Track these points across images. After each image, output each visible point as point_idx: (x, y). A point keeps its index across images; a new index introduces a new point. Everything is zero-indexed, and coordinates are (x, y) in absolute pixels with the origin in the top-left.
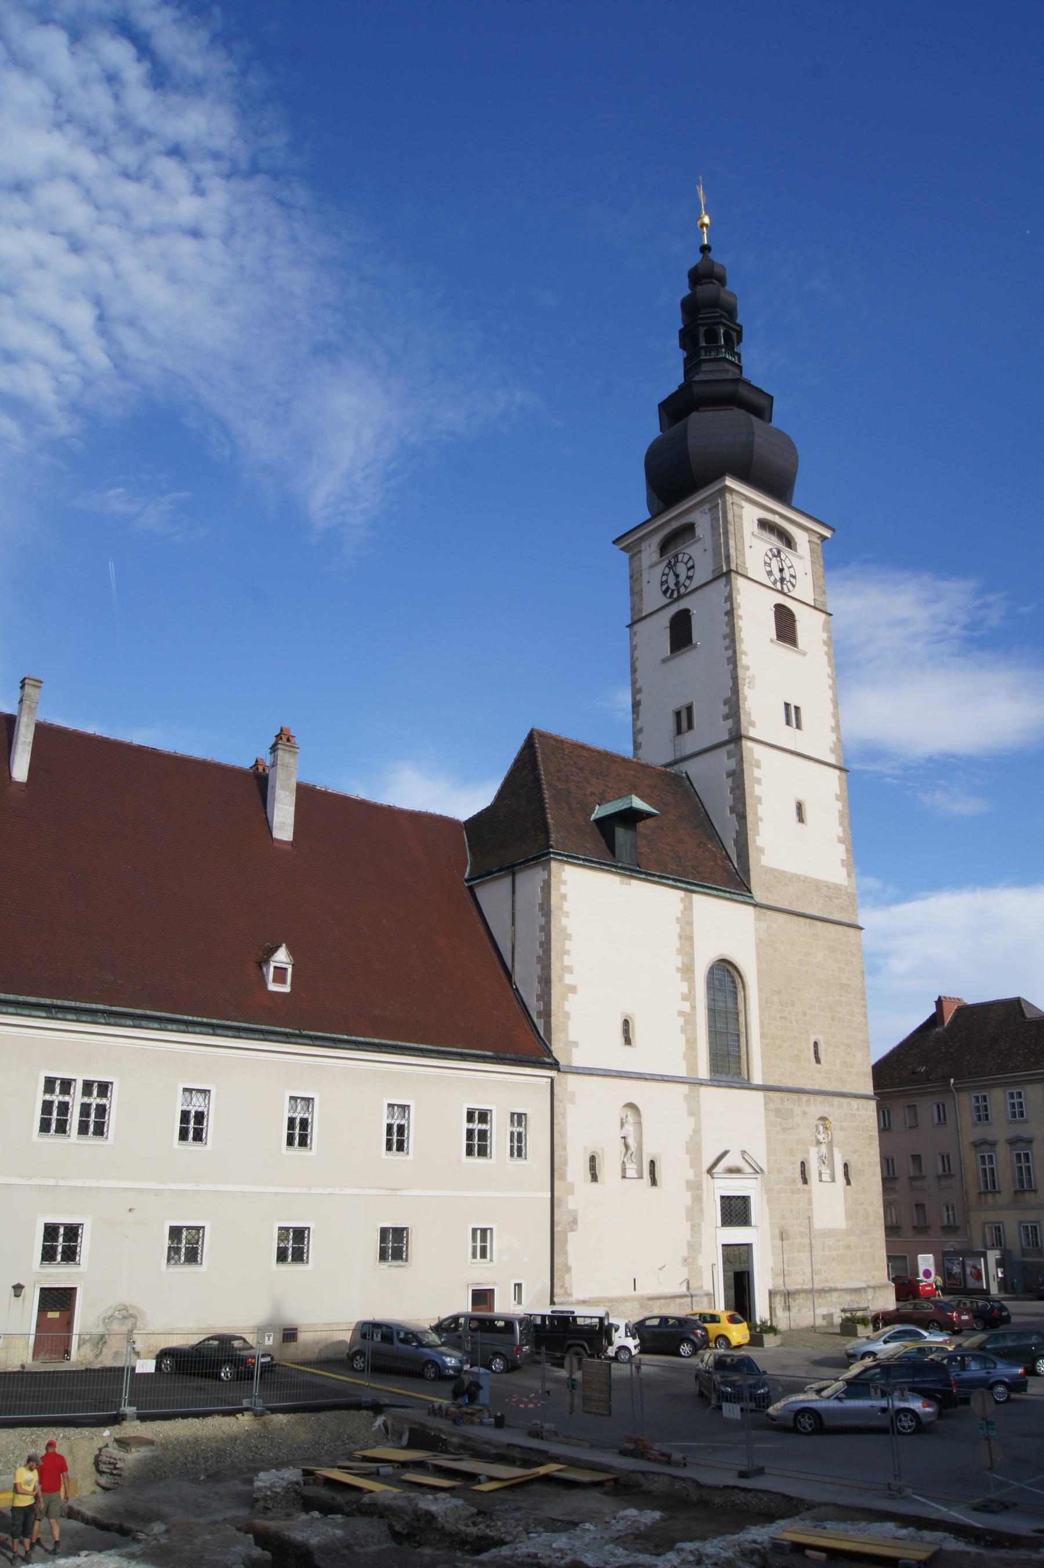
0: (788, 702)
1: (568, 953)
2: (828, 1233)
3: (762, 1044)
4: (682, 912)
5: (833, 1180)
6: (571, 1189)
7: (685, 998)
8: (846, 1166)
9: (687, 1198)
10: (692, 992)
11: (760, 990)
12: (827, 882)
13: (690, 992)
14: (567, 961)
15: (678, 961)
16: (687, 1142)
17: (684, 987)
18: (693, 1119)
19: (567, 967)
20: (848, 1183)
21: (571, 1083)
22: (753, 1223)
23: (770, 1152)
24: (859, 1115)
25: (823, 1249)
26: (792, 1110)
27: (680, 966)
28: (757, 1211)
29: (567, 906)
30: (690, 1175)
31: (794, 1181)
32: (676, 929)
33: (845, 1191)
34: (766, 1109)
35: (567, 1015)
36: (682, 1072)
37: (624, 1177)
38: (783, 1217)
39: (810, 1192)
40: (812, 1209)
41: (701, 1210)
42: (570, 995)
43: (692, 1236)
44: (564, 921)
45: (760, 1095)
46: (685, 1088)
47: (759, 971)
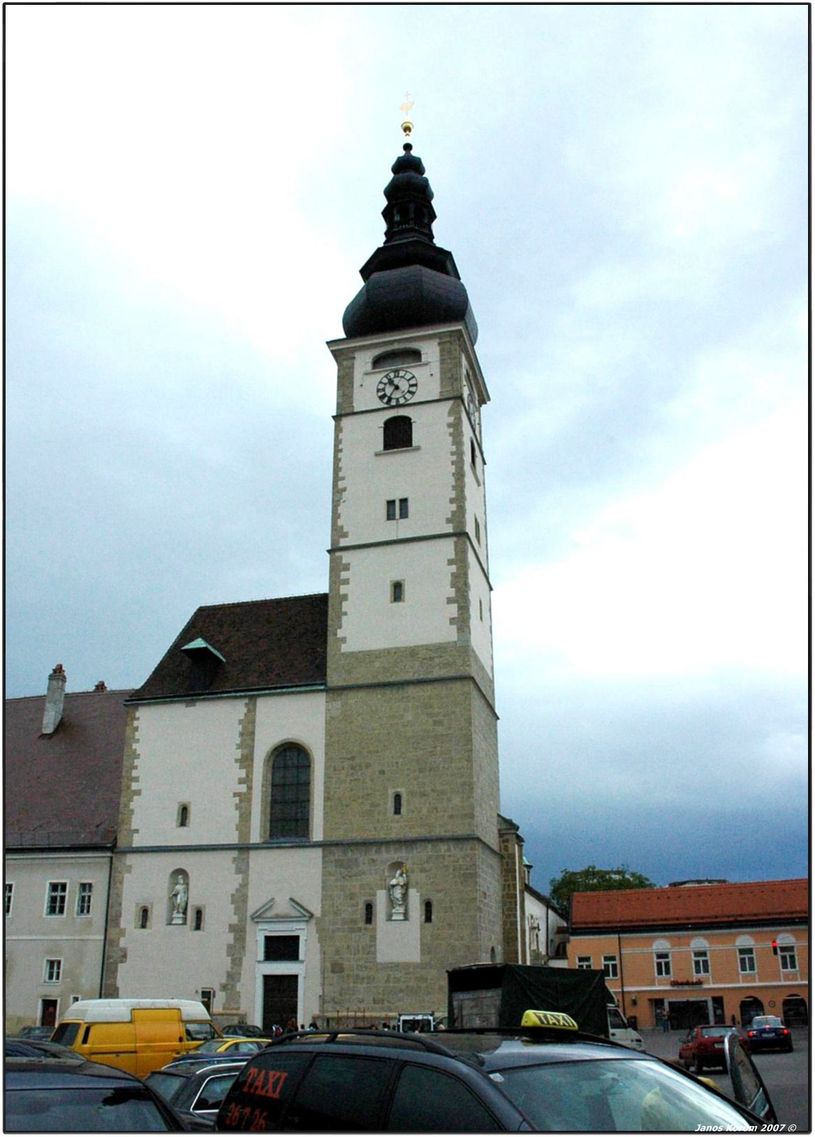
0: (391, 498)
1: (136, 768)
2: (397, 966)
3: (325, 807)
4: (246, 714)
5: (406, 916)
6: (122, 933)
7: (241, 781)
8: (428, 906)
9: (230, 938)
10: (250, 776)
11: (328, 758)
12: (426, 645)
13: (247, 776)
14: (134, 773)
15: (238, 754)
16: (233, 895)
17: (243, 773)
18: (241, 876)
19: (134, 778)
20: (428, 919)
21: (131, 859)
22: (301, 956)
23: (324, 899)
24: (450, 856)
25: (388, 981)
26: (356, 860)
27: (239, 757)
28: (309, 947)
29: (137, 735)
30: (235, 920)
31: (354, 921)
32: (240, 728)
33: (422, 928)
34: (324, 862)
35: (132, 812)
36: (234, 839)
37: (170, 924)
38: (337, 952)
39: (374, 930)
40: (375, 945)
41: (243, 948)
42: (135, 798)
43: (232, 968)
44: (134, 746)
45: (318, 853)
46: (235, 854)
47: (327, 745)
